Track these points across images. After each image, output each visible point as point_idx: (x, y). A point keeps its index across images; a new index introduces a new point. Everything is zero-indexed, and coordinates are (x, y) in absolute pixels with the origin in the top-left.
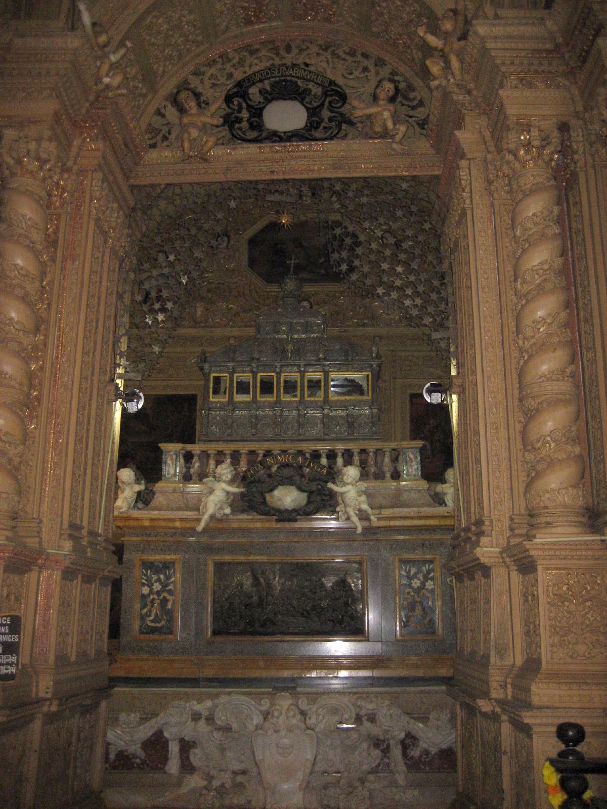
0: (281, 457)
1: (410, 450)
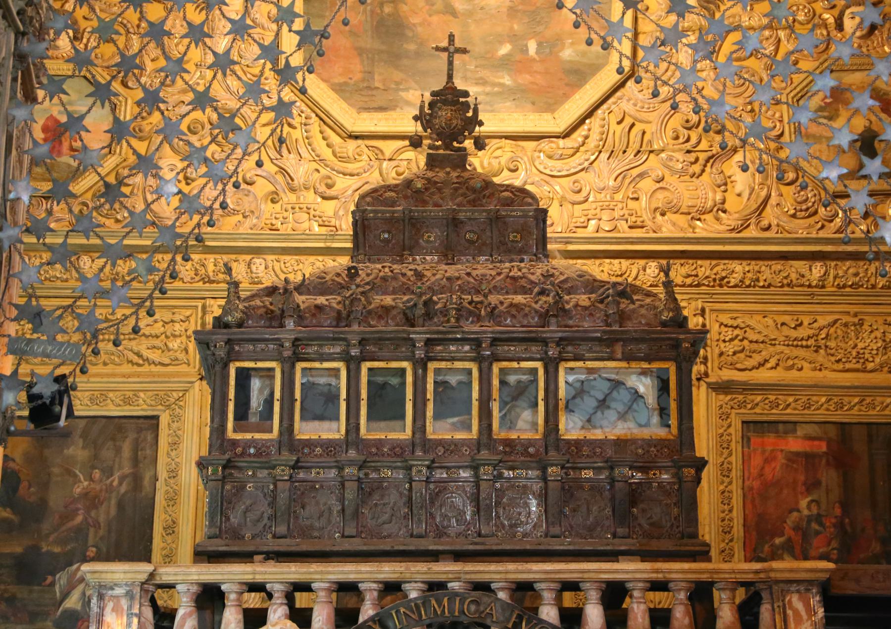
1: (794, 588)
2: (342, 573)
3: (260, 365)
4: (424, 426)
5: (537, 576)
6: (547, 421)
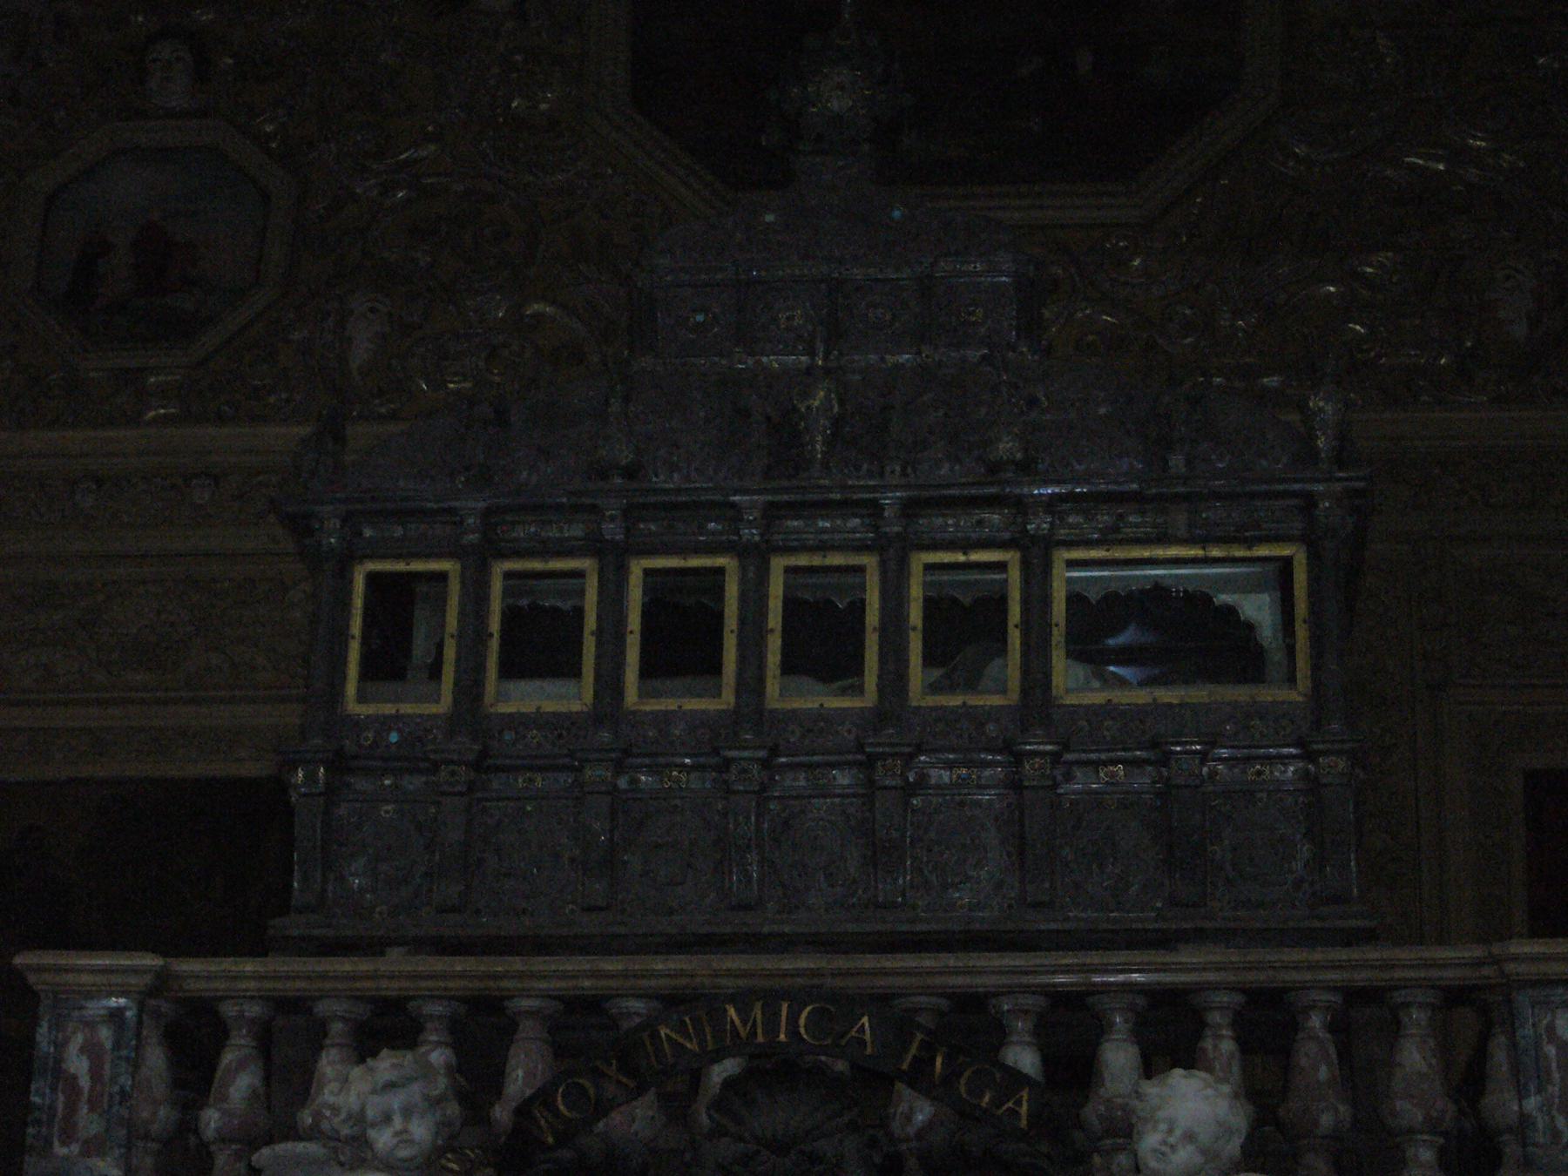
0: (744, 1012)
2: (564, 976)
3: (418, 566)
4: (761, 680)
5: (991, 981)
6: (1026, 671)
